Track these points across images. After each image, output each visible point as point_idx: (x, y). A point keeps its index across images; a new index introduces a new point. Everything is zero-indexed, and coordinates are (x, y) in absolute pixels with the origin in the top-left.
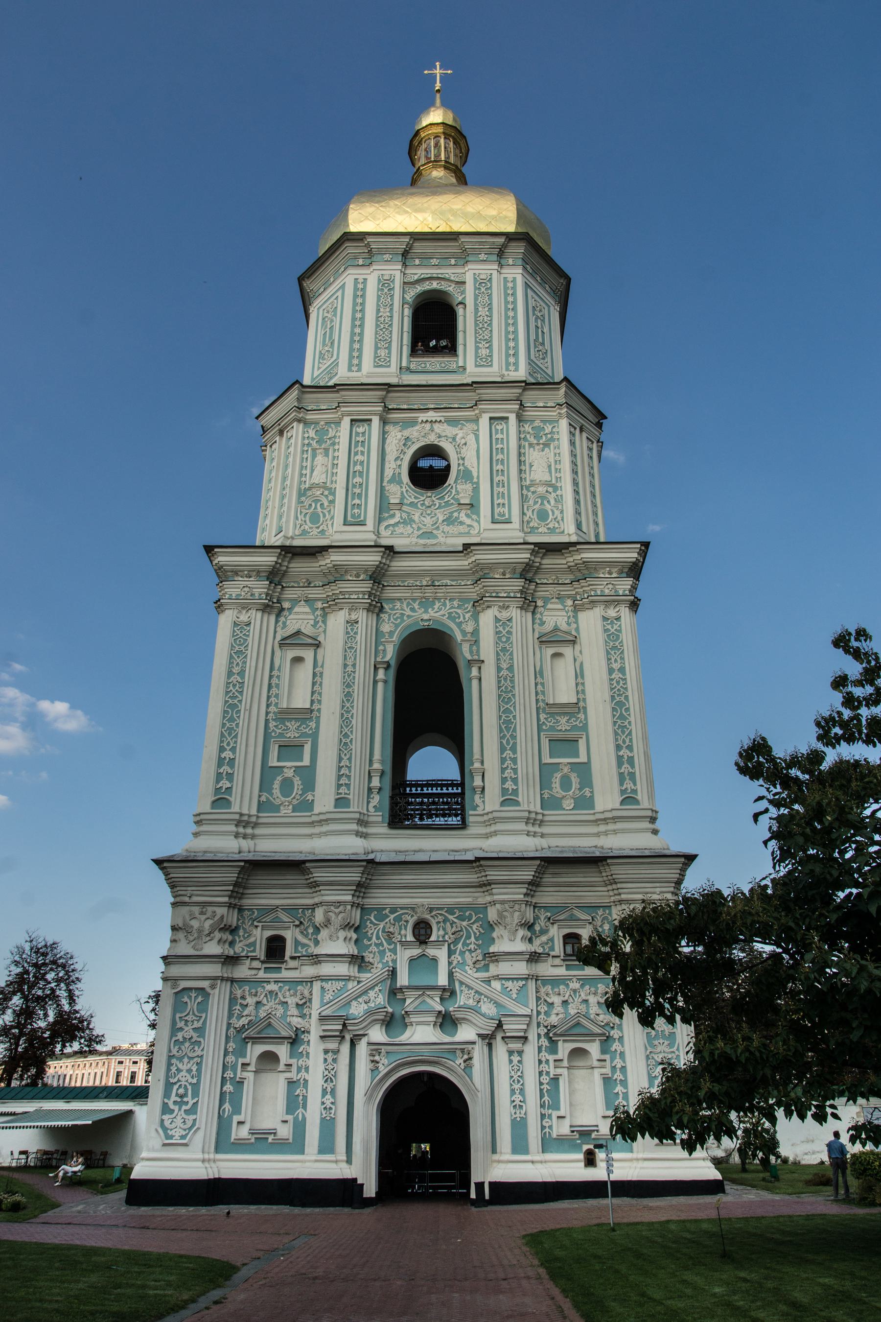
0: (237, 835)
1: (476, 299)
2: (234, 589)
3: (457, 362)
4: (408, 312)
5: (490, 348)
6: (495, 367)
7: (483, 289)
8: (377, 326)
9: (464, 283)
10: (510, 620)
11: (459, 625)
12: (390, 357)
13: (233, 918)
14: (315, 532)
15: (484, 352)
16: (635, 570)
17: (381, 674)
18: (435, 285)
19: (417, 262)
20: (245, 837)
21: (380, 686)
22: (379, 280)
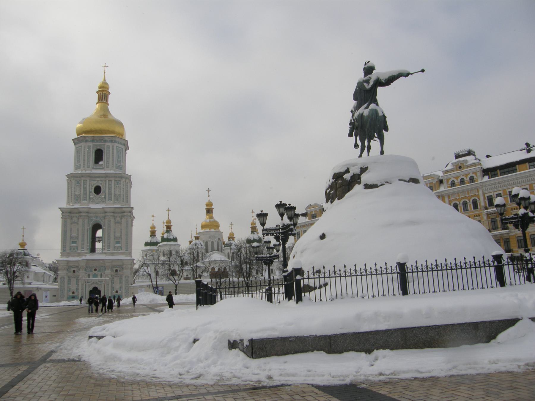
2: (64, 214)
4: (94, 154)
18: (99, 147)
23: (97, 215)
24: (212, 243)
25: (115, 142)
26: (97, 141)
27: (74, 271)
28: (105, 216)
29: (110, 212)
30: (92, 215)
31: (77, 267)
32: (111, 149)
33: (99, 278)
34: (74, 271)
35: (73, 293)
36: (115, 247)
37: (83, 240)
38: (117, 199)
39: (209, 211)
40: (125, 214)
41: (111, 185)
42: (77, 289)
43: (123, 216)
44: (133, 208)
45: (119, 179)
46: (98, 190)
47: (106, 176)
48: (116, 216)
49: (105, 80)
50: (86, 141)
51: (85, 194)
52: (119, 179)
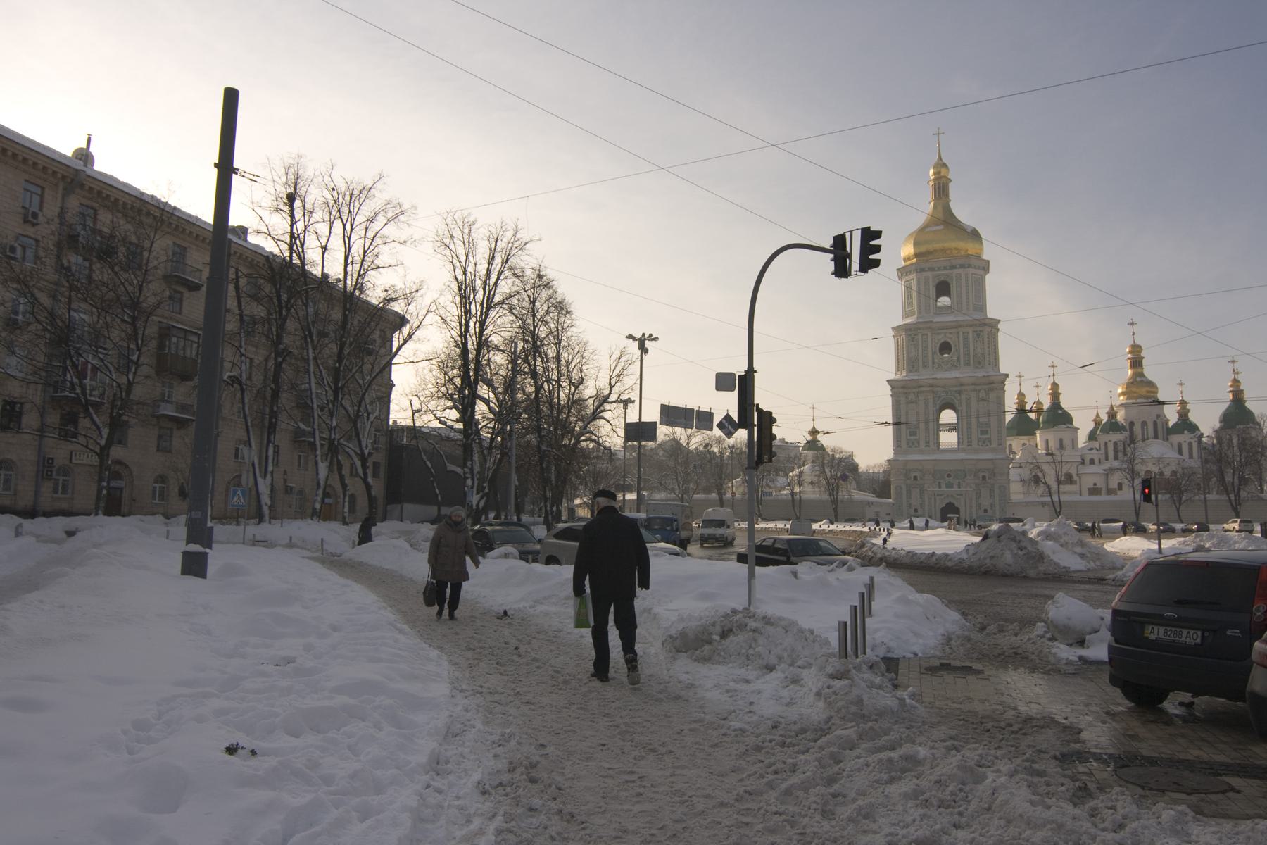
16: (1003, 382)
24: (1144, 424)
25: (969, 266)
26: (939, 269)
27: (915, 478)
32: (963, 280)
33: (956, 488)
34: (915, 478)
36: (979, 440)
38: (979, 364)
39: (1137, 363)
42: (922, 506)
43: (992, 390)
44: (1007, 376)
46: (945, 348)
49: (940, 158)
50: (922, 270)
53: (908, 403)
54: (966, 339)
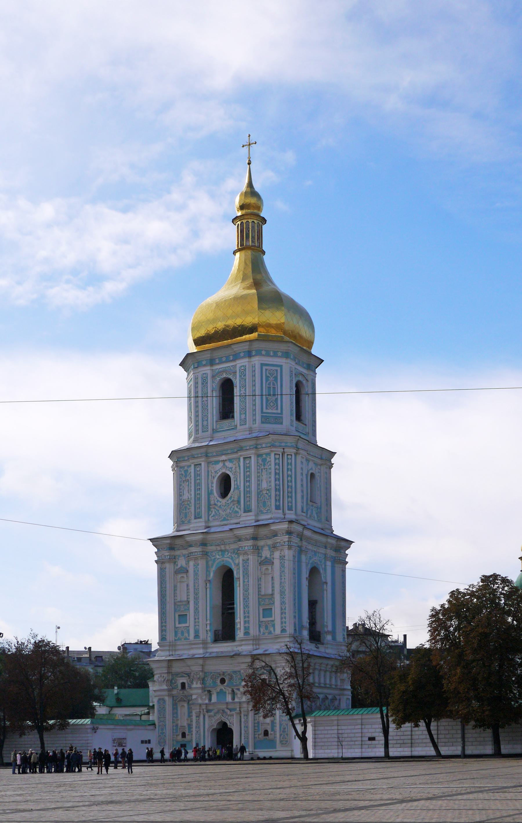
0: (169, 650)
1: (240, 383)
3: (234, 421)
5: (245, 414)
6: (247, 426)
7: (242, 377)
8: (202, 407)
9: (236, 372)
10: (248, 560)
11: (233, 560)
12: (207, 425)
13: (170, 677)
14: (186, 522)
15: (243, 416)
17: (208, 584)
18: (224, 376)
19: (217, 361)
20: (172, 650)
21: (208, 590)
22: (202, 378)
23: (223, 547)
25: (259, 353)
26: (221, 363)
28: (238, 550)
29: (247, 539)
30: (213, 548)
31: (188, 675)
34: (183, 685)
35: (184, 735)
37: (196, 610)
40: (278, 539)
41: (249, 467)
42: (190, 726)
45: (267, 450)
46: (225, 485)
47: (237, 446)
48: (262, 547)
50: (199, 365)
51: (198, 499)
52: (267, 450)
53: (177, 572)
54: (247, 468)
